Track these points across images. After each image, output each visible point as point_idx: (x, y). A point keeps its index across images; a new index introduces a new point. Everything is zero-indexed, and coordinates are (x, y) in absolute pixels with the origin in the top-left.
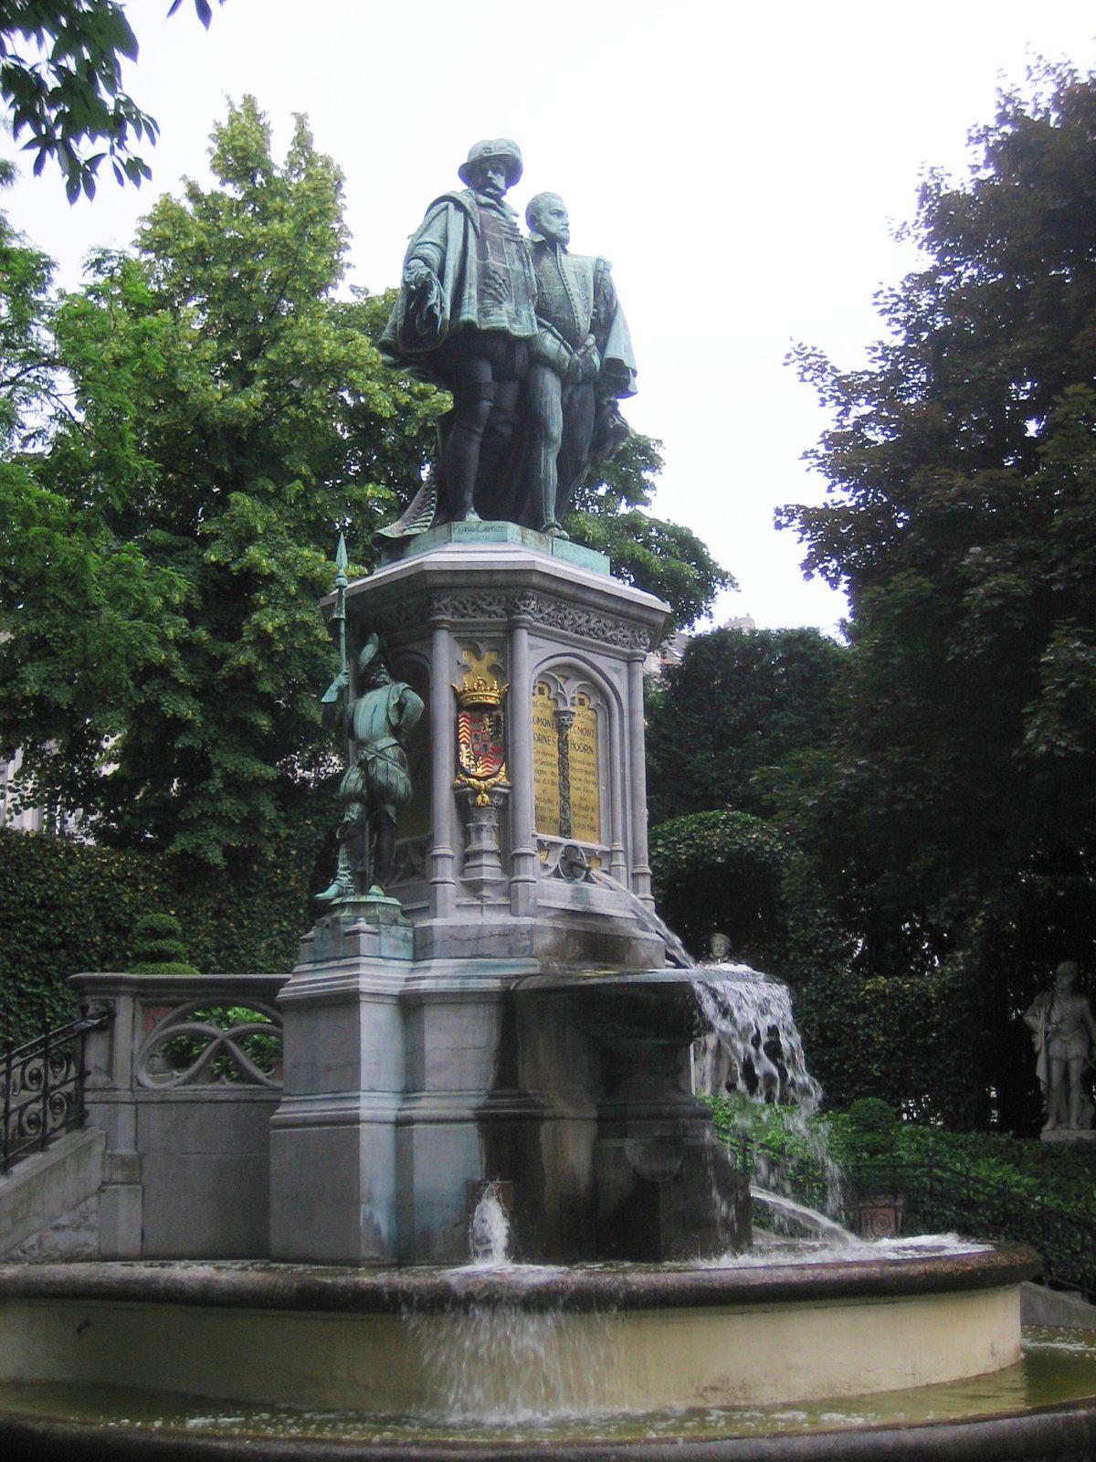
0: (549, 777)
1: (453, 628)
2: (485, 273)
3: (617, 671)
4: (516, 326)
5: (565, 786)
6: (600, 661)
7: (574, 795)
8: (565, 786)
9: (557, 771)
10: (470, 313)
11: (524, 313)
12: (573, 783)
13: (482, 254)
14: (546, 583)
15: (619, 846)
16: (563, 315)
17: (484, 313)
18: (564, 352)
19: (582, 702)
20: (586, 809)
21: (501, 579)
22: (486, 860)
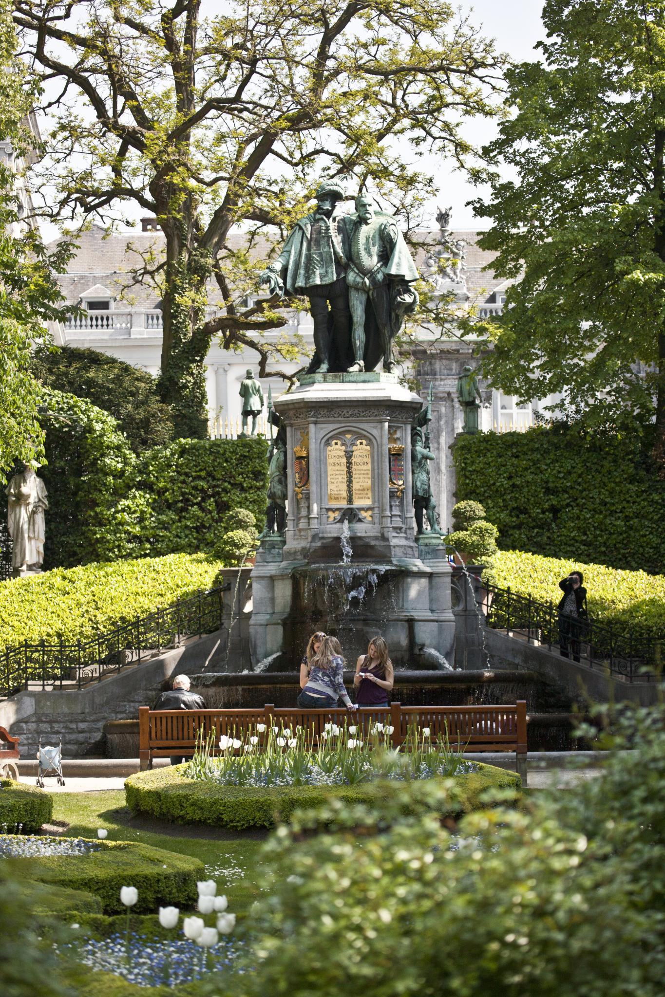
0: (340, 480)
1: (291, 425)
2: (309, 258)
3: (375, 428)
4: (326, 279)
5: (350, 481)
6: (362, 426)
7: (356, 486)
8: (350, 481)
9: (345, 477)
10: (300, 283)
11: (330, 271)
12: (354, 481)
13: (309, 248)
14: (314, 405)
15: (376, 505)
16: (357, 261)
17: (307, 278)
18: (358, 279)
19: (361, 443)
20: (364, 490)
21: (297, 406)
22: (302, 520)
